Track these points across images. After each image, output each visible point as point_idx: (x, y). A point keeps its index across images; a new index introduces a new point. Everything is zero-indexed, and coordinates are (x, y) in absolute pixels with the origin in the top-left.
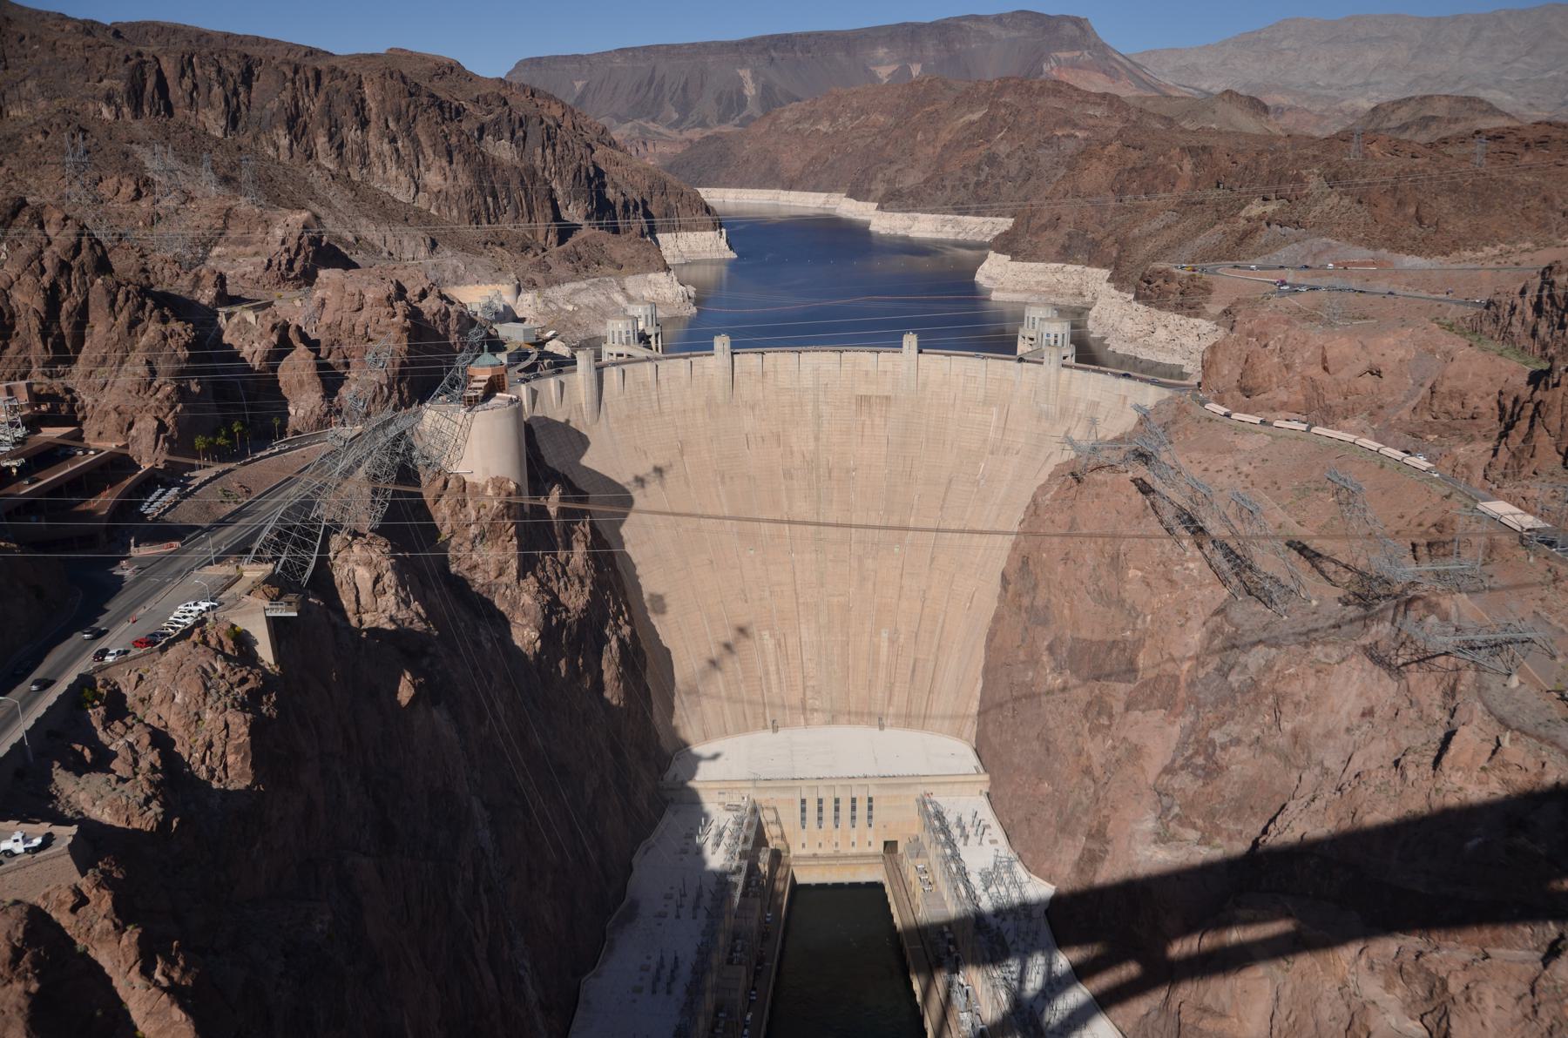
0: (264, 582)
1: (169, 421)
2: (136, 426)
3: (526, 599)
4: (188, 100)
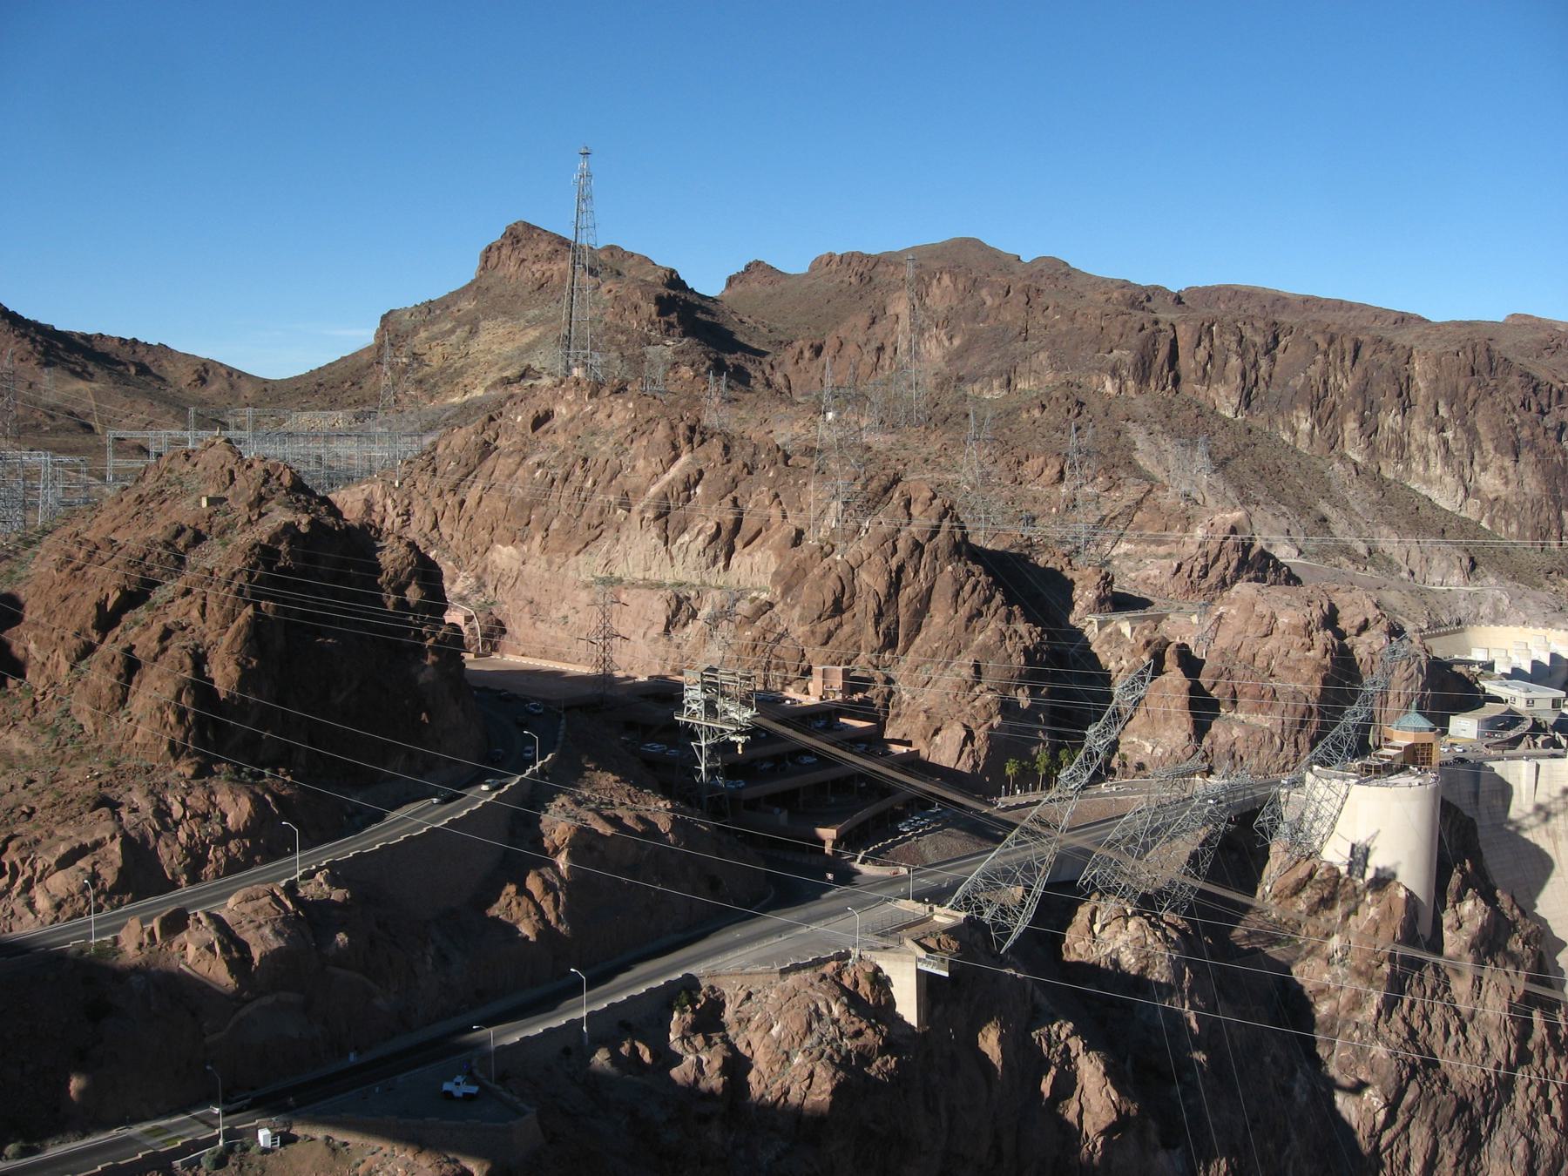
0: (944, 932)
1: (981, 734)
2: (942, 733)
3: (1379, 1050)
4: (1200, 374)
